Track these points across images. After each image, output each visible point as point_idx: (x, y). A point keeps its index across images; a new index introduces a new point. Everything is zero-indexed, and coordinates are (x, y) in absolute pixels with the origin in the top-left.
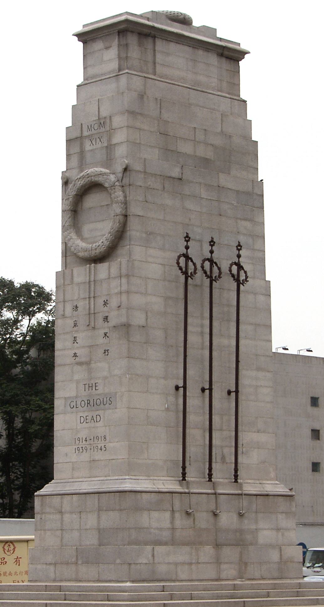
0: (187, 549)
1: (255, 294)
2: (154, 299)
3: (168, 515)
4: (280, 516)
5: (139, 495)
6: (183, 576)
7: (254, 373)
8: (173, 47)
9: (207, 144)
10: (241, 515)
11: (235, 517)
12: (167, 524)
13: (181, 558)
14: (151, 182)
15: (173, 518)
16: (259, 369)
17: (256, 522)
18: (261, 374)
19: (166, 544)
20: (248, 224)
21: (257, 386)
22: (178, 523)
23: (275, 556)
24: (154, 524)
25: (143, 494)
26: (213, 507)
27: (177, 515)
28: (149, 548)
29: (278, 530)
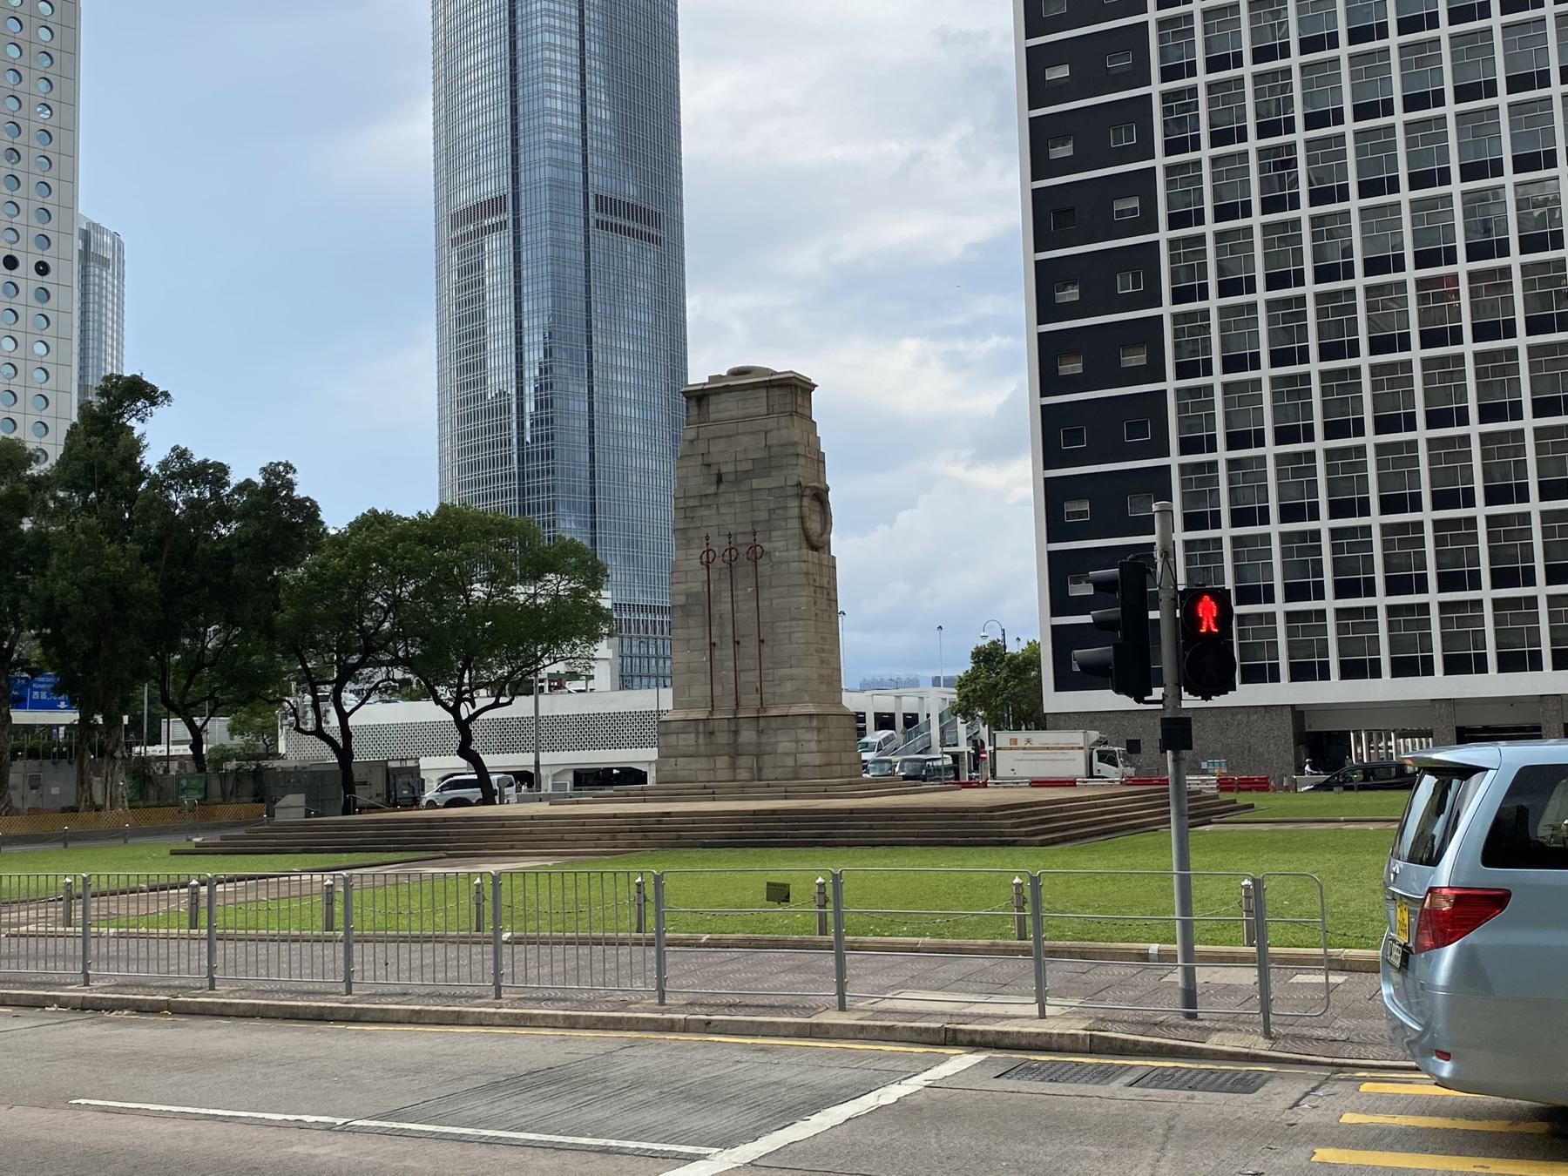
0: (703, 759)
1: (788, 563)
2: (693, 585)
3: (693, 735)
4: (799, 731)
5: (668, 724)
6: (701, 779)
7: (787, 624)
8: (723, 397)
9: (746, 460)
10: (760, 732)
12: (693, 742)
13: (700, 766)
14: (691, 503)
15: (697, 737)
16: (791, 620)
18: (793, 623)
19: (692, 756)
20: (781, 511)
21: (790, 633)
22: (701, 741)
23: (790, 762)
24: (681, 743)
25: (673, 724)
26: (733, 728)
27: (701, 736)
28: (673, 760)
29: (797, 742)
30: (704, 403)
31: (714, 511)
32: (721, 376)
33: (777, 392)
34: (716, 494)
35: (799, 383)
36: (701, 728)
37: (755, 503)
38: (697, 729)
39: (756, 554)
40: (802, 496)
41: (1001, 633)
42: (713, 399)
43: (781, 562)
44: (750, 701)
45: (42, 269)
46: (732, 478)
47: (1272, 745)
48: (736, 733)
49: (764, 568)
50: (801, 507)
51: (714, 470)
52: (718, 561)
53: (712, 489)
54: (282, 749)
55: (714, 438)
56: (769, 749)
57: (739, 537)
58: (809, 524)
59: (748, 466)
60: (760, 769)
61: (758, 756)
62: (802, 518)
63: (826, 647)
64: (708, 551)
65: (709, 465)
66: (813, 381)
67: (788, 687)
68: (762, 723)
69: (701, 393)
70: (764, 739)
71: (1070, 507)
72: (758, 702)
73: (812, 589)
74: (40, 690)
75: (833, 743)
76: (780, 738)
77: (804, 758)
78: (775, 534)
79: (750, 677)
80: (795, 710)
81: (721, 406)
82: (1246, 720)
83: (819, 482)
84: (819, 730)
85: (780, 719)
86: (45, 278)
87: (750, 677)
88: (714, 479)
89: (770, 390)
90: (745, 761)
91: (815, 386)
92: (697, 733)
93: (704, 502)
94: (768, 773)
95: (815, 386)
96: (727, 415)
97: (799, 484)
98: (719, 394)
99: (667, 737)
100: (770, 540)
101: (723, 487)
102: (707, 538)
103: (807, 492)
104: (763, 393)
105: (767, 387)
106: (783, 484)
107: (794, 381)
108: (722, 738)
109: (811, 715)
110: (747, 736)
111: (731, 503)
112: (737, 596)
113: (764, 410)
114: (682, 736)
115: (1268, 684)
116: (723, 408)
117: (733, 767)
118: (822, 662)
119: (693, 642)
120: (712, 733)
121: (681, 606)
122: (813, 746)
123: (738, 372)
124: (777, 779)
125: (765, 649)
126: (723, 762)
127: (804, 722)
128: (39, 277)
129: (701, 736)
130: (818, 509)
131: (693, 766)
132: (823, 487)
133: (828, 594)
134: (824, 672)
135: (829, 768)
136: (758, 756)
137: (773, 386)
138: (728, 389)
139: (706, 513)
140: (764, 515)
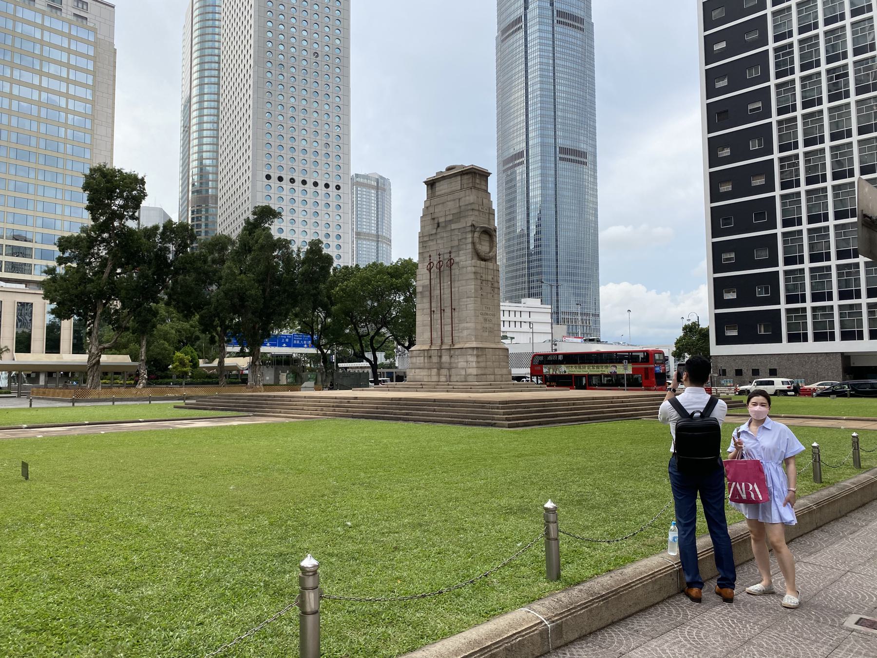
0: (426, 370)
3: (422, 358)
6: (425, 380)
7: (465, 300)
11: (448, 357)
13: (425, 374)
14: (426, 239)
15: (424, 359)
16: (468, 297)
17: (458, 359)
18: (468, 299)
20: (464, 240)
22: (426, 361)
24: (418, 361)
26: (439, 355)
27: (426, 358)
29: (467, 362)
30: (434, 187)
31: (435, 242)
32: (441, 172)
33: (466, 177)
34: (436, 234)
35: (477, 171)
36: (426, 354)
37: (453, 237)
38: (424, 354)
39: (451, 263)
40: (474, 232)
41: (697, 318)
42: (437, 184)
43: (463, 267)
44: (448, 340)
45: (338, 187)
46: (443, 224)
47: (830, 373)
48: (440, 357)
49: (455, 271)
50: (473, 237)
51: (436, 221)
52: (434, 269)
53: (434, 231)
54: (397, 365)
55: (436, 205)
56: (454, 365)
57: (445, 255)
58: (478, 247)
59: (450, 218)
60: (450, 376)
61: (449, 369)
62: (473, 243)
63: (488, 312)
64: (431, 263)
65: (434, 219)
66: (489, 171)
67: (465, 333)
68: (452, 352)
69: (432, 182)
70: (453, 360)
71: (724, 256)
72: (451, 341)
73: (479, 281)
74: (297, 340)
75: (488, 363)
76: (460, 360)
77: (470, 371)
78: (461, 252)
79: (448, 328)
80: (467, 345)
81: (441, 187)
82: (815, 360)
83: (489, 225)
84: (478, 356)
85: (459, 350)
86: (339, 191)
87: (448, 328)
88: (436, 226)
89: (463, 176)
90: (444, 372)
91: (490, 174)
92: (424, 357)
93: (431, 238)
94: (454, 378)
95: (490, 174)
96: (443, 192)
97: (473, 225)
98: (440, 181)
99: (412, 358)
100: (458, 256)
101: (439, 230)
102: (430, 256)
103: (478, 229)
104: (459, 178)
105: (461, 175)
106: (465, 226)
107: (473, 170)
108: (435, 360)
109: (473, 348)
110: (445, 358)
111: (442, 238)
112: (444, 286)
113: (460, 188)
114: (418, 358)
115: (829, 342)
116: (442, 188)
117: (439, 375)
118: (485, 320)
119: (425, 310)
120: (430, 357)
121: (421, 292)
122: (474, 364)
123: (449, 169)
124: (457, 382)
125: (455, 314)
126: (434, 371)
127: (470, 352)
128: (337, 191)
129: (426, 358)
130: (488, 239)
131: (422, 374)
132: (492, 227)
133: (492, 284)
134: (487, 325)
135: (485, 376)
136: (449, 369)
137: (464, 174)
138: (444, 178)
139: (432, 244)
140: (456, 243)
